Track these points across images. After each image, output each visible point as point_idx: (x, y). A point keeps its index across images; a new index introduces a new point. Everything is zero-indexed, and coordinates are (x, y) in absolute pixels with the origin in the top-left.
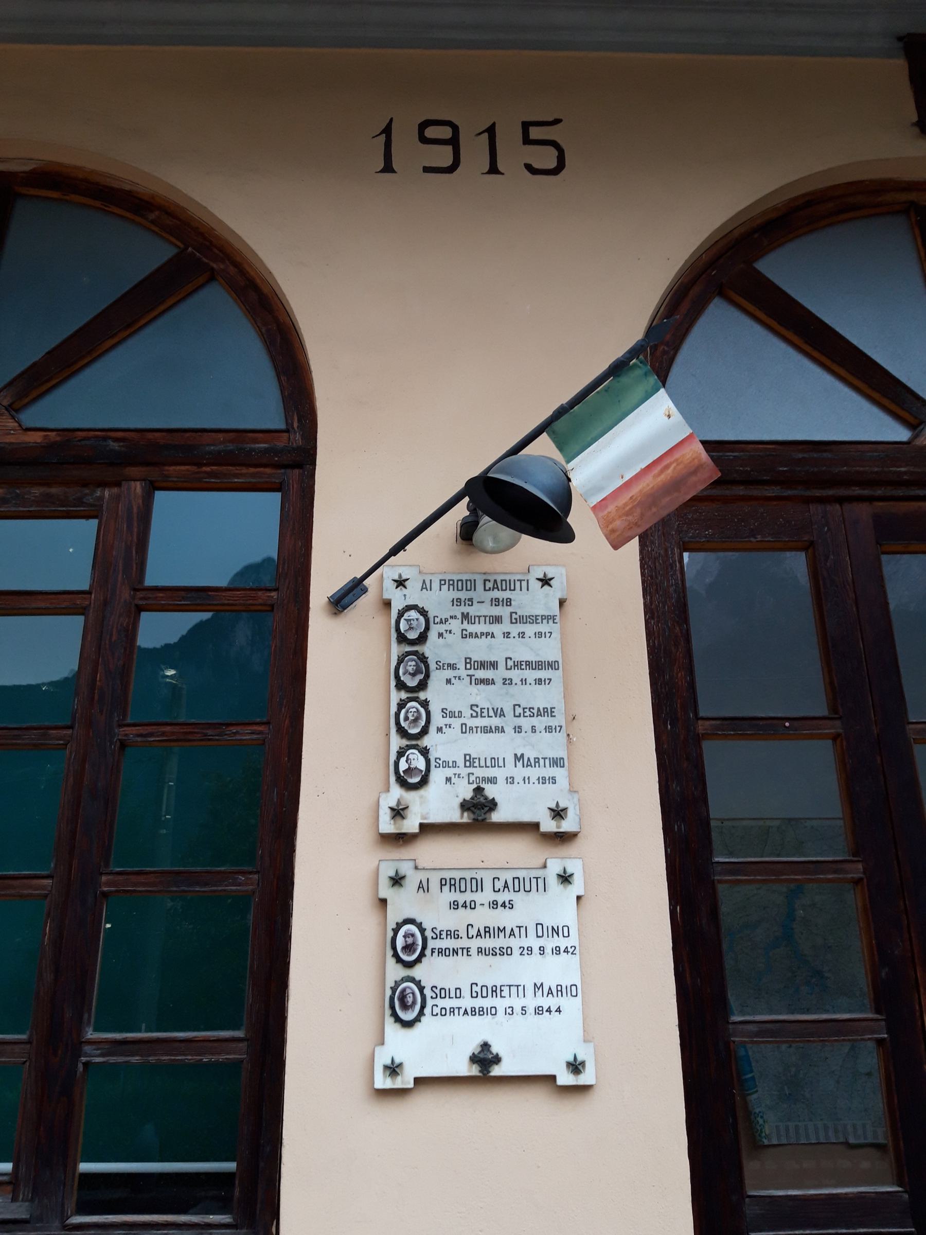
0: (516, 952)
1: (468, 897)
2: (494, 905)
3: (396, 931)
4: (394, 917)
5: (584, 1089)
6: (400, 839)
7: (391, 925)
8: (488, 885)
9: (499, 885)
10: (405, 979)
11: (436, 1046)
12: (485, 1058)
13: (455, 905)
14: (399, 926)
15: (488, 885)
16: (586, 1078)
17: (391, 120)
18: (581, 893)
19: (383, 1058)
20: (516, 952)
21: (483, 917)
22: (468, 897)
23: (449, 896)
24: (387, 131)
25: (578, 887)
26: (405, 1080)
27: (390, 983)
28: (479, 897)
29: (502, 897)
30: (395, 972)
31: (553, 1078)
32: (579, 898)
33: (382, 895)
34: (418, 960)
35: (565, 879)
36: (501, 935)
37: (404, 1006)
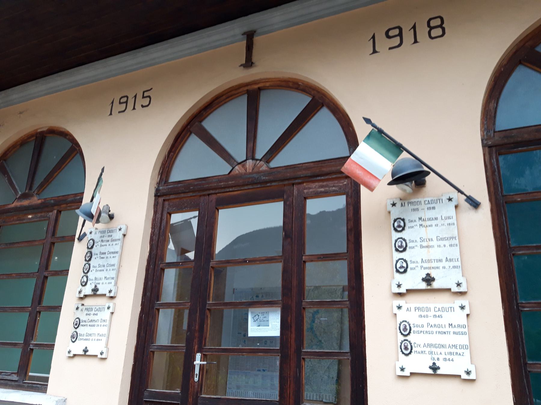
0: (452, 333)
1: (425, 313)
2: (435, 316)
3: (400, 325)
4: (399, 320)
5: (473, 381)
6: (400, 295)
7: (399, 322)
8: (432, 309)
9: (437, 309)
10: (405, 340)
11: (419, 363)
12: (434, 368)
13: (421, 316)
14: (401, 323)
15: (432, 309)
16: (472, 376)
17: (374, 34)
18: (469, 313)
19: (399, 365)
20: (452, 333)
21: (433, 321)
22: (425, 313)
23: (418, 313)
24: (373, 37)
25: (467, 311)
26: (407, 373)
27: (399, 342)
28: (429, 313)
29: (438, 314)
30: (402, 338)
31: (460, 376)
32: (468, 315)
33: (394, 312)
34: (409, 334)
35: (462, 308)
36: (451, 327)
37: (407, 350)
